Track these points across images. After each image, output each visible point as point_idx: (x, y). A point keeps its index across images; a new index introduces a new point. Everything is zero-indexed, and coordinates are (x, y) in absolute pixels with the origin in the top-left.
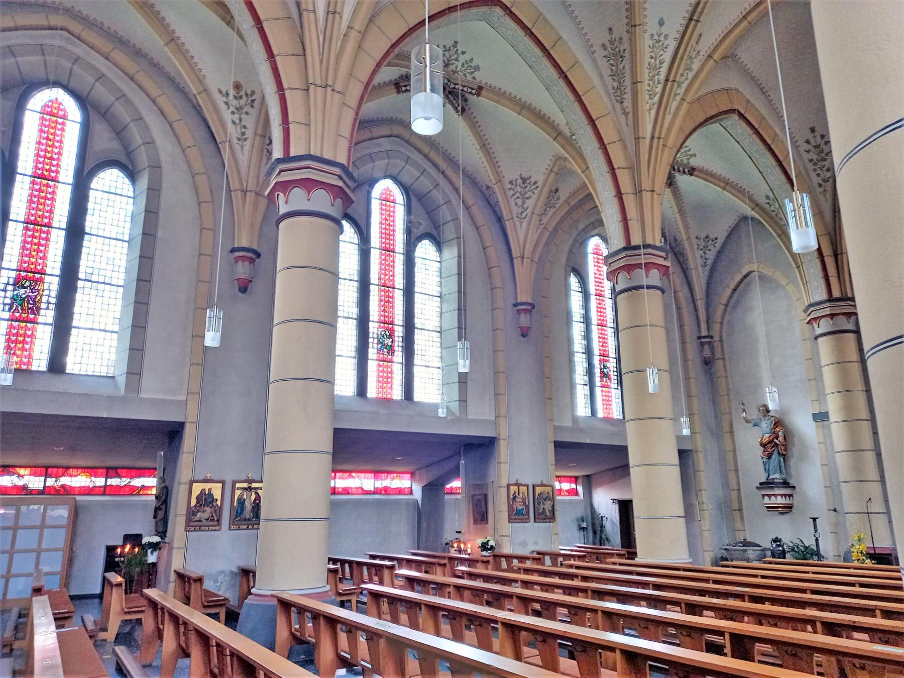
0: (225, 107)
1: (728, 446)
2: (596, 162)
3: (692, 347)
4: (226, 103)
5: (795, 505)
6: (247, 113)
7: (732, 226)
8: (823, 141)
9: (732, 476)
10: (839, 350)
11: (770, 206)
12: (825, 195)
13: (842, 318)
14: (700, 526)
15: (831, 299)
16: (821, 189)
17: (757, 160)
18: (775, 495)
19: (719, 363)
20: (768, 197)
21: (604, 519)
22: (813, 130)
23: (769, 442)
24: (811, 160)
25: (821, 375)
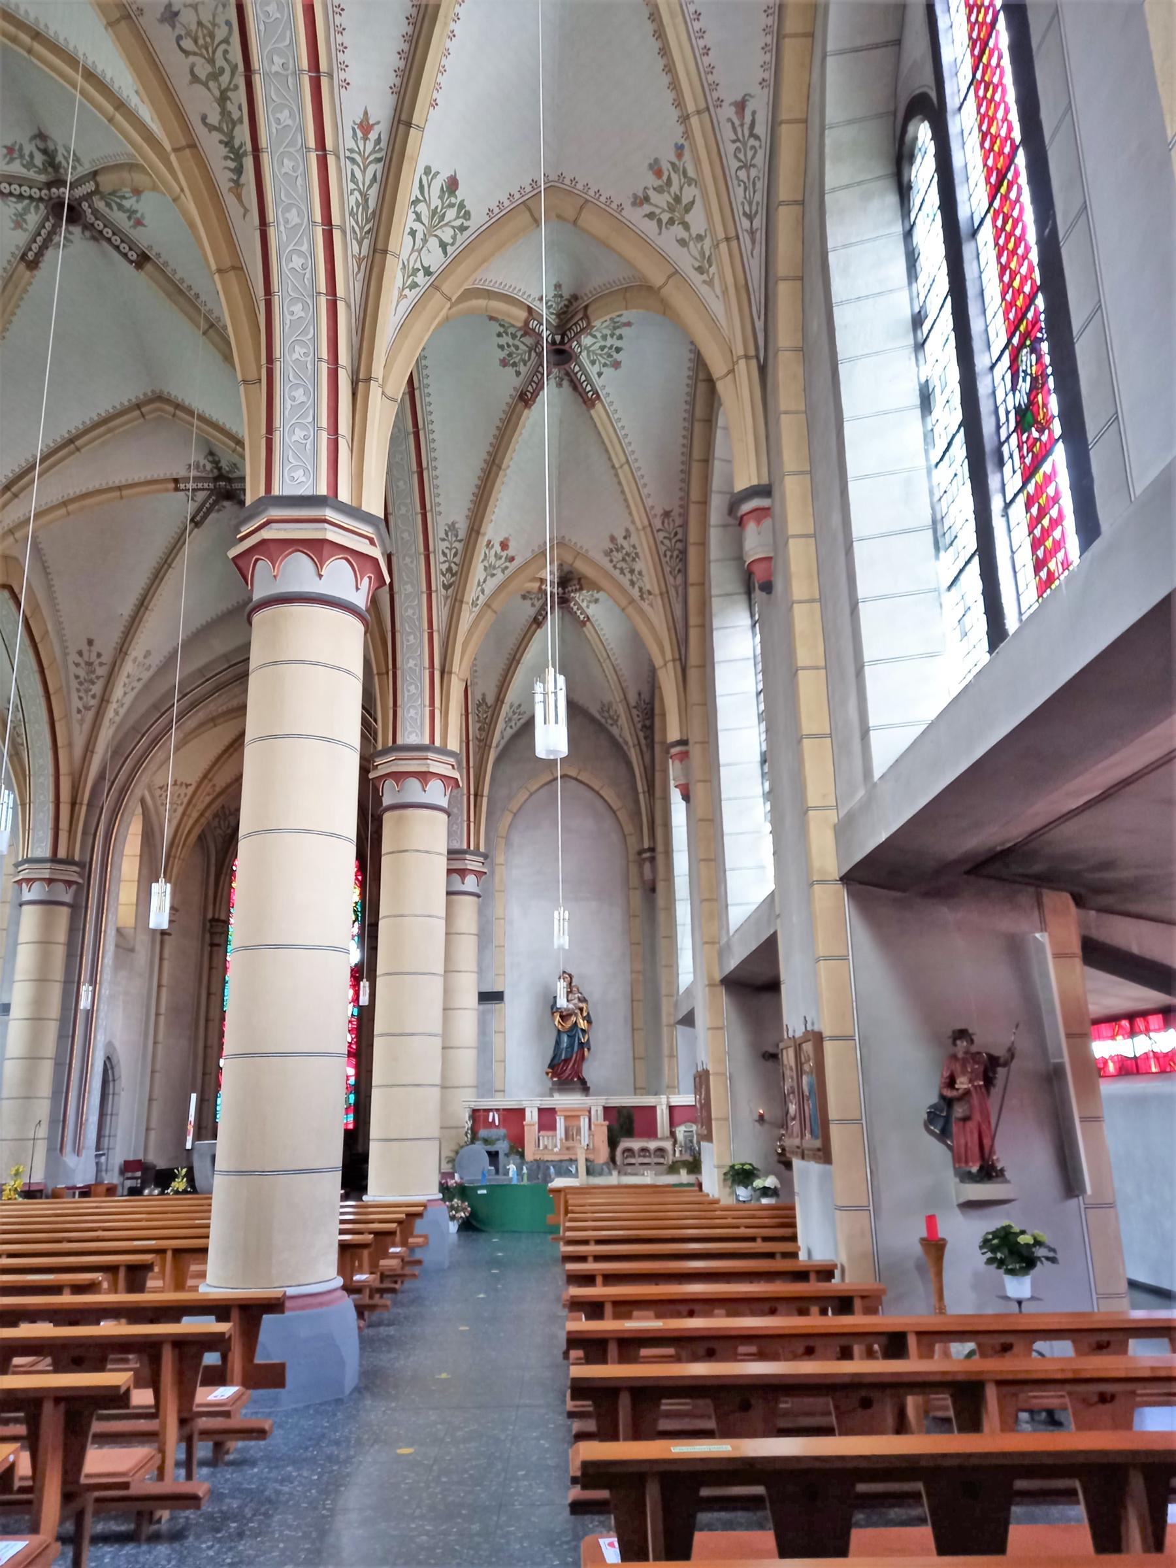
8: (99, 660)
10: (47, 926)
12: (81, 725)
13: (61, 887)
15: (54, 859)
16: (79, 716)
22: (90, 642)
24: (77, 677)
25: (14, 954)
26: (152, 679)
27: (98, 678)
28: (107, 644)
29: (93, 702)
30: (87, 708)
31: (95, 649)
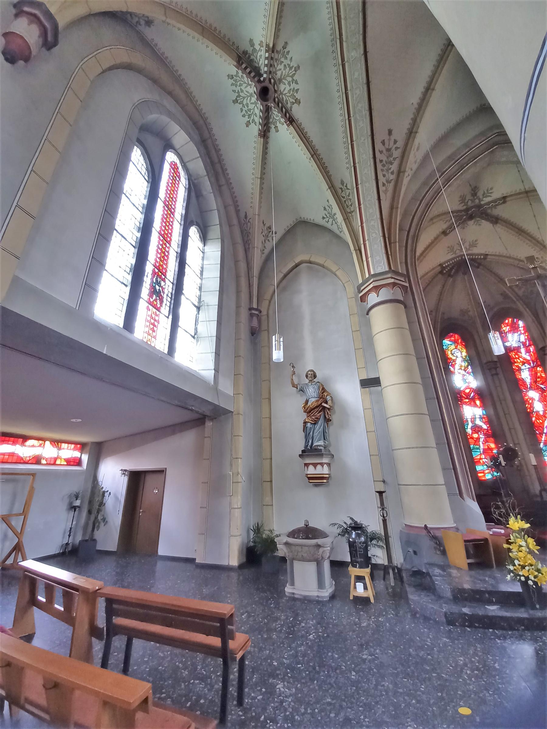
1: (265, 414)
3: (244, 314)
5: (332, 475)
7: (290, 227)
8: (395, 146)
9: (265, 443)
11: (342, 191)
12: (386, 194)
14: (230, 503)
16: (384, 188)
17: (356, 120)
18: (322, 464)
19: (264, 335)
20: (342, 183)
21: (106, 494)
22: (390, 132)
23: (317, 407)
24: (381, 161)
26: (418, 169)
27: (395, 159)
28: (400, 135)
29: (392, 177)
30: (389, 182)
31: (393, 138)
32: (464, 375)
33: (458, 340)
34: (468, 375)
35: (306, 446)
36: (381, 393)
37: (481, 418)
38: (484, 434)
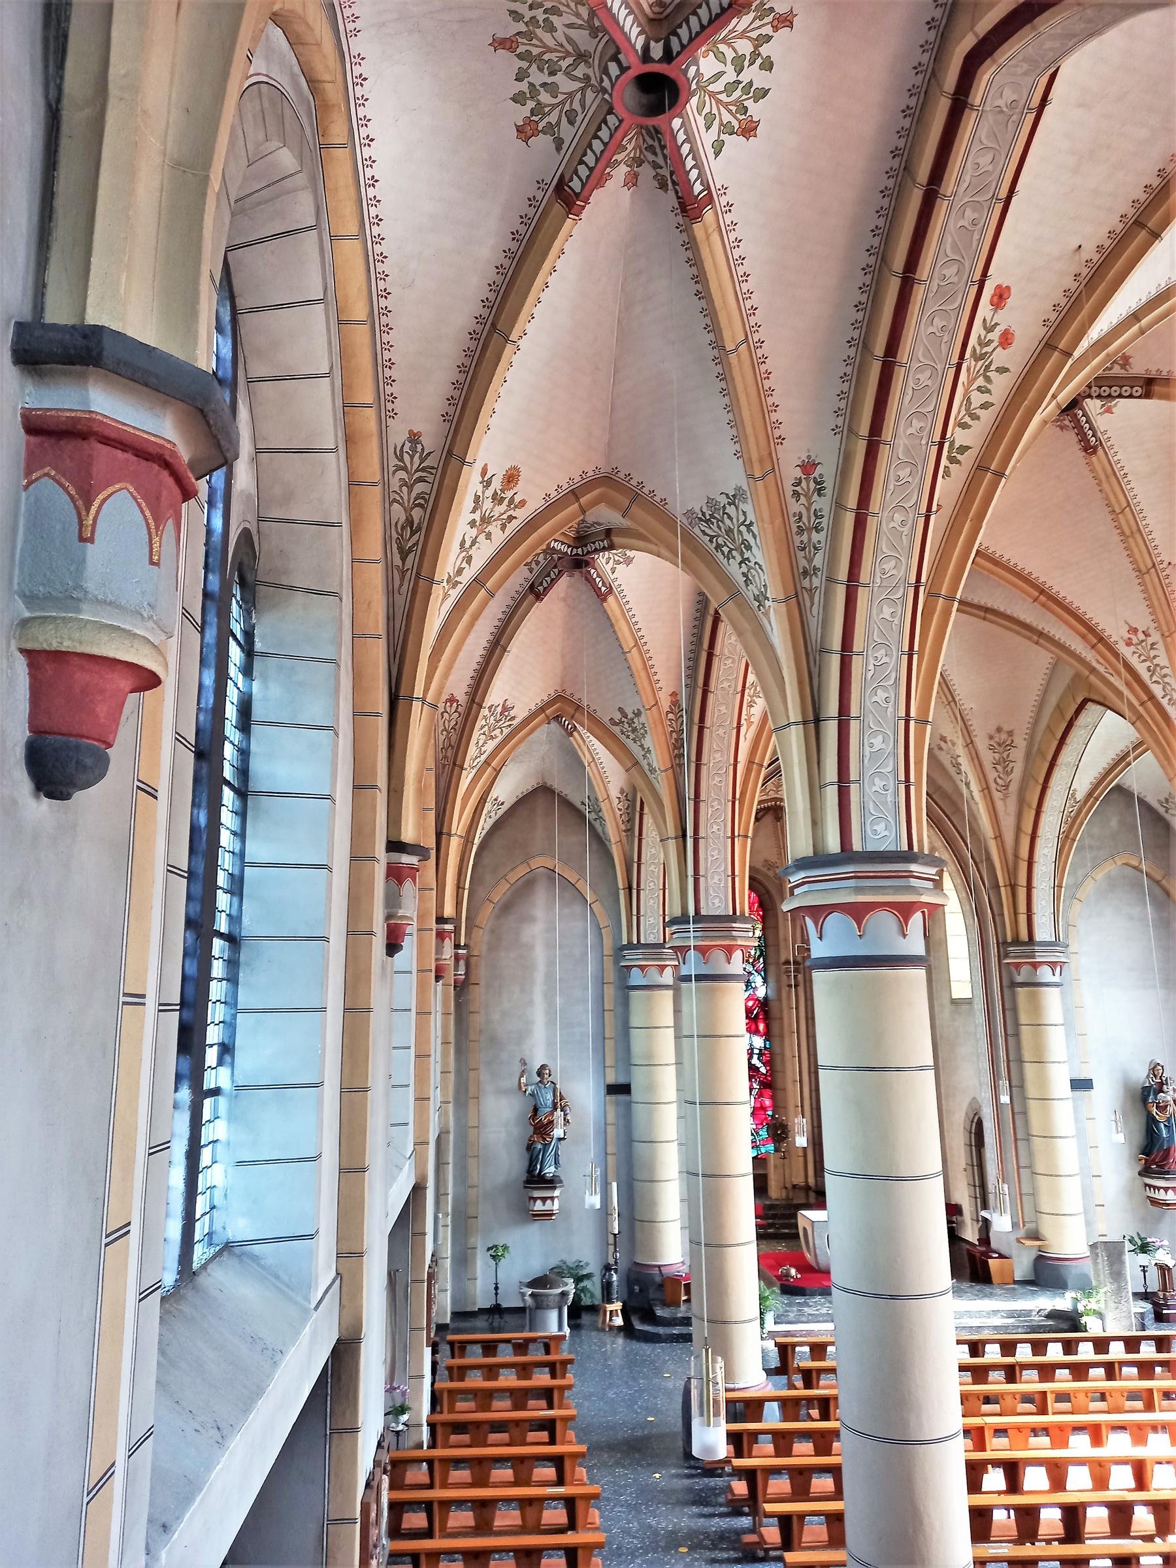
0: (469, 503)
2: (717, 779)
4: (477, 499)
6: (489, 536)
18: (552, 1198)
32: (750, 973)
33: (753, 903)
34: (756, 974)
35: (530, 1170)
36: (628, 1106)
37: (760, 1054)
38: (761, 1083)
